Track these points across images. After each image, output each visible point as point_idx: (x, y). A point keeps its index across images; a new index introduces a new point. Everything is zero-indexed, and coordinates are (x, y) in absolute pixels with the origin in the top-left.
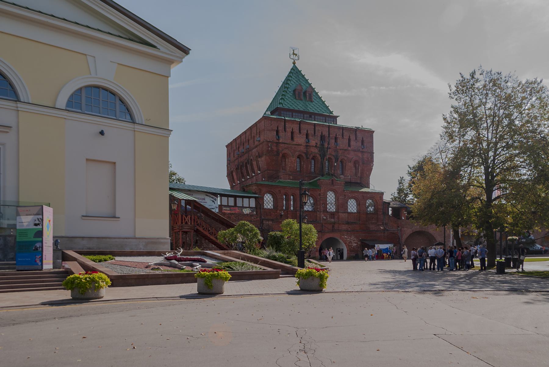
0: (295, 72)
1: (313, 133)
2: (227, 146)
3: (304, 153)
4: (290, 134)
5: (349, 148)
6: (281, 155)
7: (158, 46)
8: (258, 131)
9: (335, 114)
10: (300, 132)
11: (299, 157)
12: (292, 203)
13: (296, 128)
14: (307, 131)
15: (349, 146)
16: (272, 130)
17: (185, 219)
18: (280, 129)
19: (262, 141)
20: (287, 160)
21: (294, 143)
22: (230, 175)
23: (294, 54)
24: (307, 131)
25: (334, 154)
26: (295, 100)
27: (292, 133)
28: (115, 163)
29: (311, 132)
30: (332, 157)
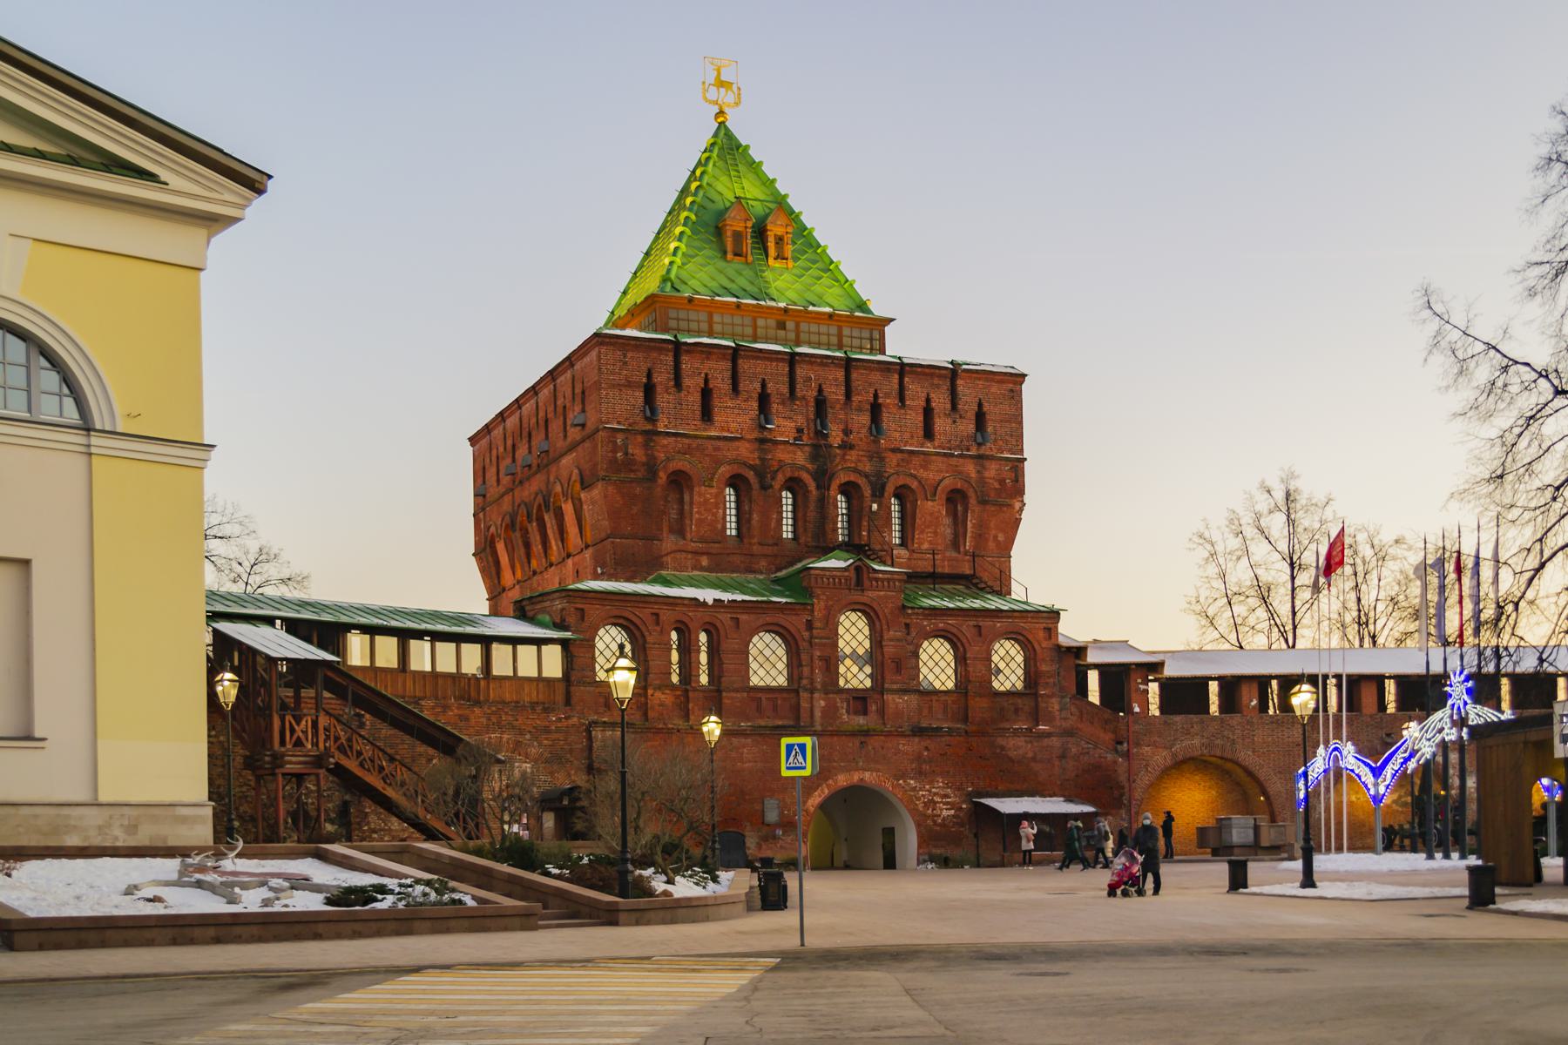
0: (727, 148)
1: (785, 390)
2: (473, 440)
3: (752, 467)
5: (929, 448)
6: (663, 477)
7: (164, 175)
8: (578, 390)
9: (878, 310)
11: (736, 482)
12: (703, 658)
14: (764, 385)
15: (929, 434)
16: (630, 385)
17: (293, 731)
18: (657, 379)
19: (590, 426)
20: (686, 498)
22: (485, 552)
23: (721, 84)
24: (764, 385)
25: (867, 467)
26: (722, 264)
27: (706, 393)
28: (26, 563)
29: (778, 387)
30: (862, 481)
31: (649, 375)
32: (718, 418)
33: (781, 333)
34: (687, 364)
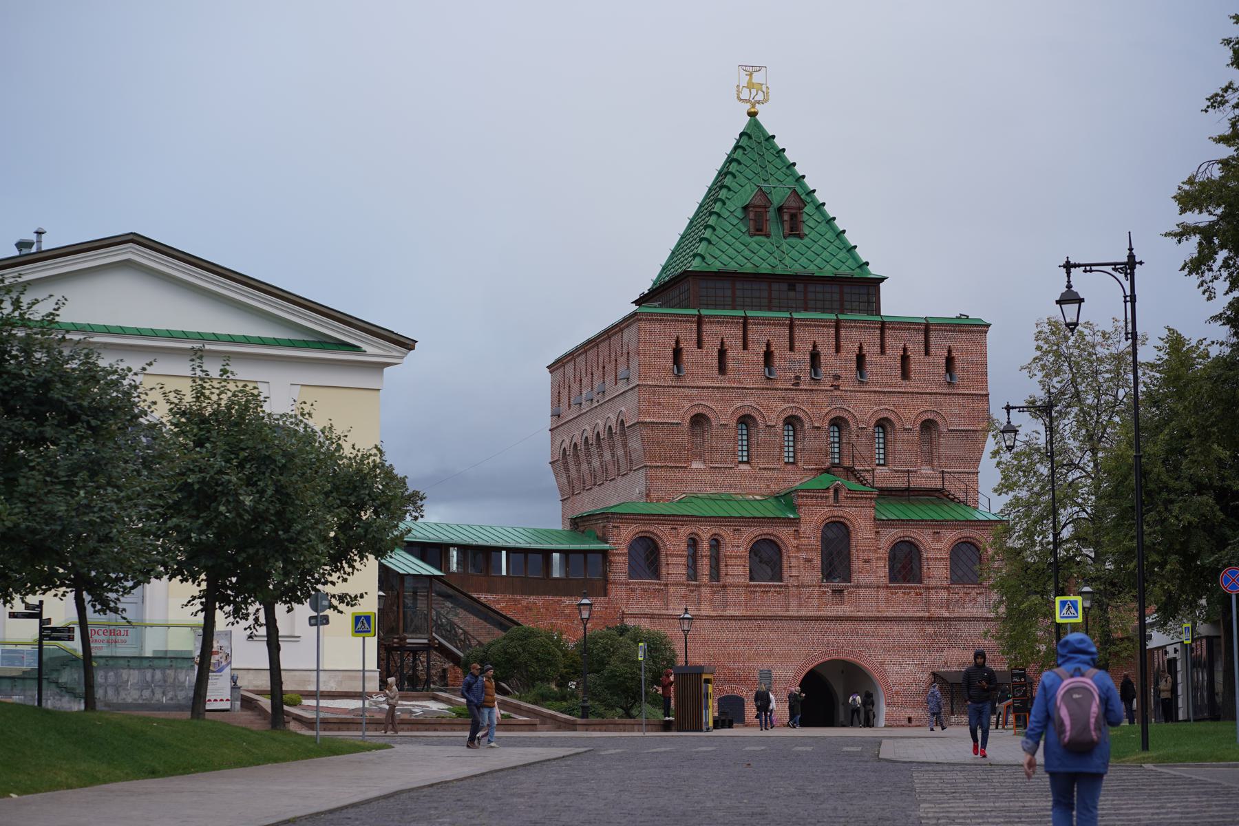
4: (715, 354)
5: (906, 386)
8: (625, 351)
9: (874, 270)
13: (732, 335)
33: (792, 294)
34: (707, 329)
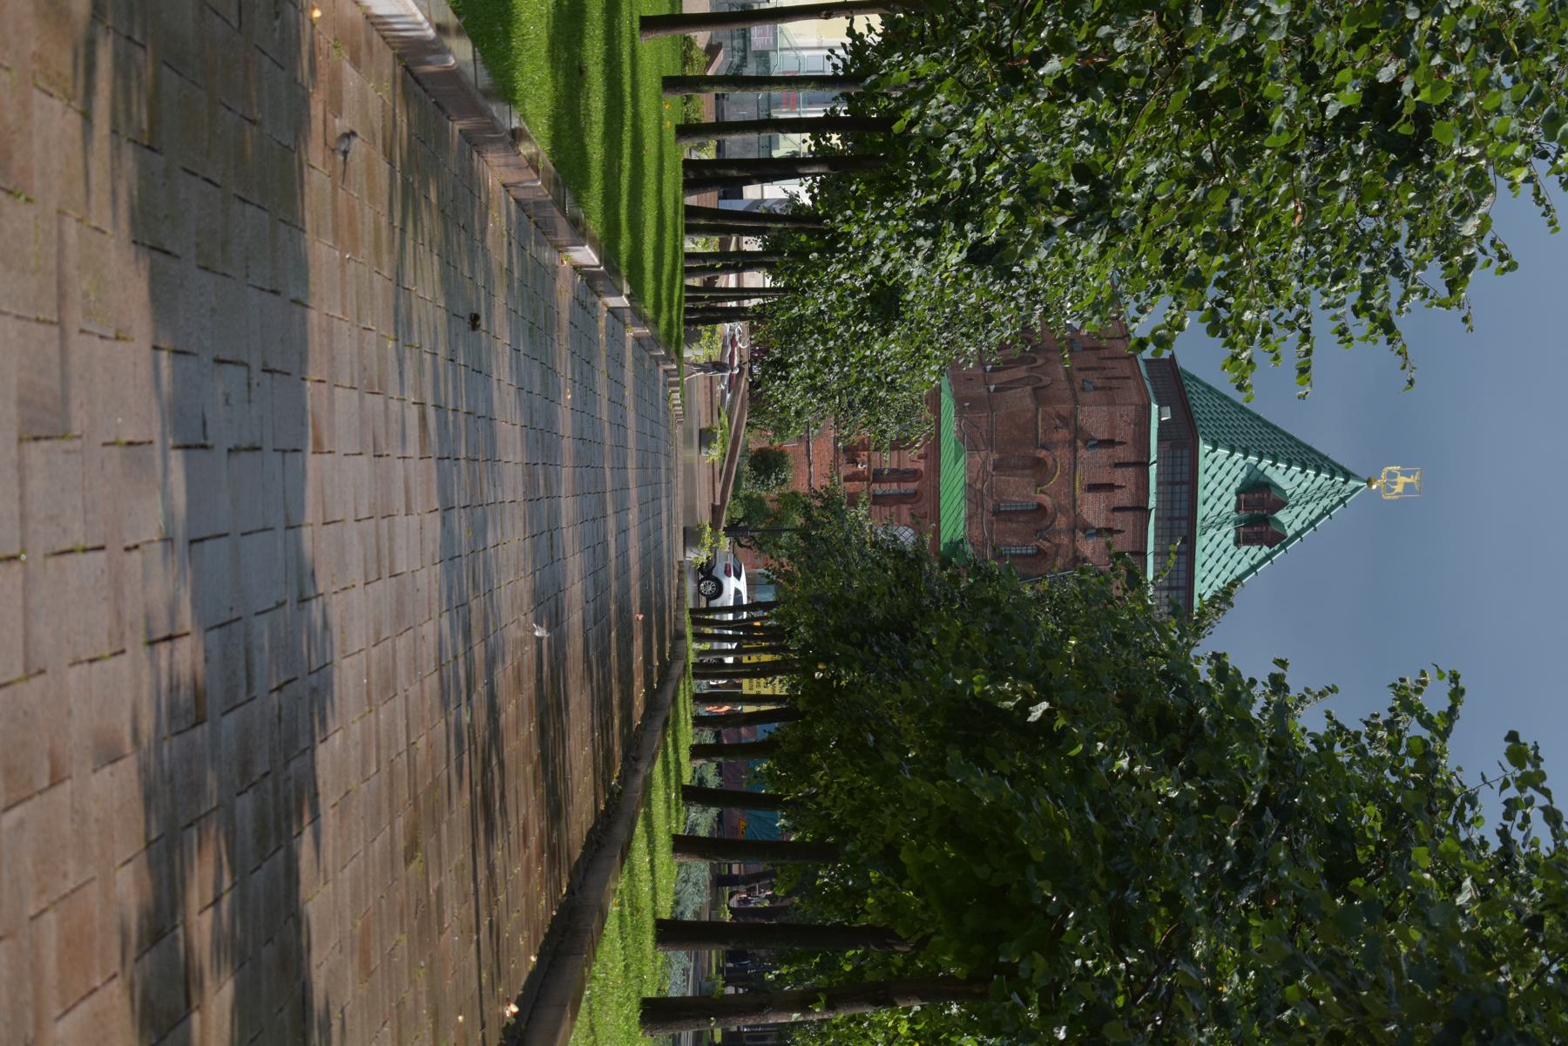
6: (1042, 454)
10: (1116, 509)
14: (1119, 532)
16: (1113, 427)
18: (1119, 449)
19: (1082, 396)
20: (1027, 472)
21: (1078, 492)
24: (1119, 532)
27: (1110, 487)
31: (1121, 443)
32: (1090, 496)
34: (1130, 472)
